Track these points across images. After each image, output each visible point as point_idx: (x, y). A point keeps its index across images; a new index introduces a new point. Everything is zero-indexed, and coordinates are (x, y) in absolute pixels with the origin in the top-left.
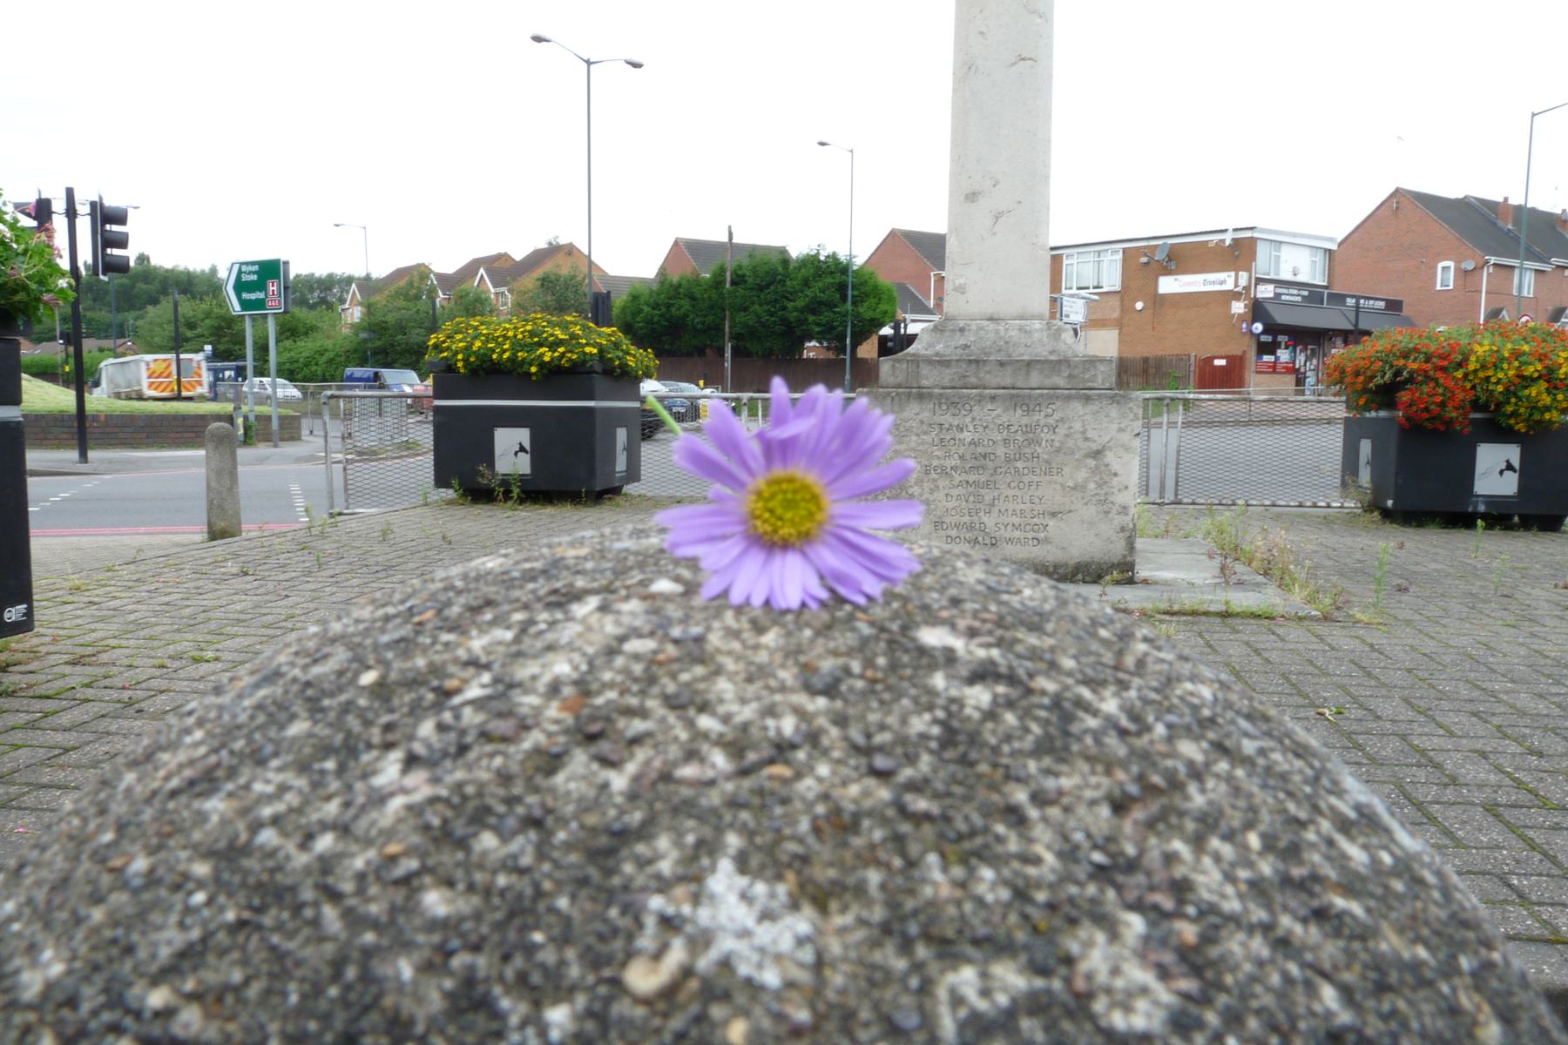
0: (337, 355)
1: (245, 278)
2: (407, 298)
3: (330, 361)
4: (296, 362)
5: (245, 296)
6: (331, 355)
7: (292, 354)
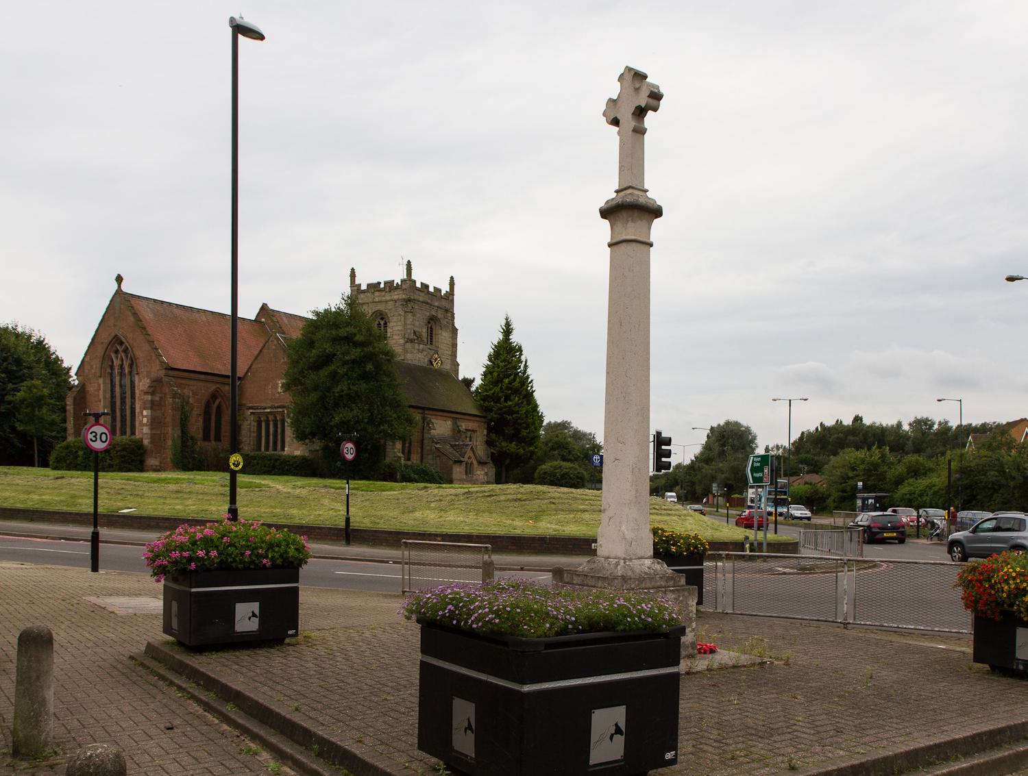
0: (940, 489)
1: (755, 465)
2: (990, 447)
3: (936, 493)
4: (914, 493)
5: (755, 475)
6: (936, 488)
7: (912, 488)
